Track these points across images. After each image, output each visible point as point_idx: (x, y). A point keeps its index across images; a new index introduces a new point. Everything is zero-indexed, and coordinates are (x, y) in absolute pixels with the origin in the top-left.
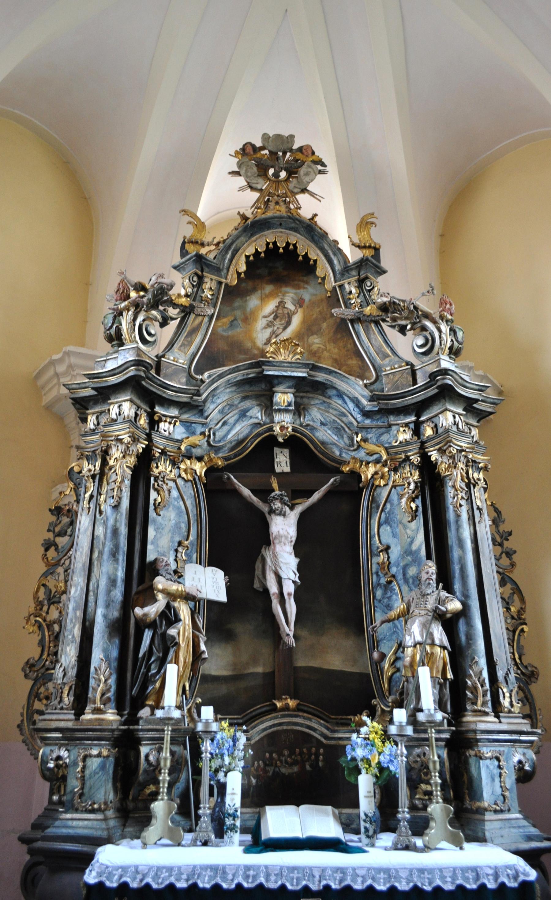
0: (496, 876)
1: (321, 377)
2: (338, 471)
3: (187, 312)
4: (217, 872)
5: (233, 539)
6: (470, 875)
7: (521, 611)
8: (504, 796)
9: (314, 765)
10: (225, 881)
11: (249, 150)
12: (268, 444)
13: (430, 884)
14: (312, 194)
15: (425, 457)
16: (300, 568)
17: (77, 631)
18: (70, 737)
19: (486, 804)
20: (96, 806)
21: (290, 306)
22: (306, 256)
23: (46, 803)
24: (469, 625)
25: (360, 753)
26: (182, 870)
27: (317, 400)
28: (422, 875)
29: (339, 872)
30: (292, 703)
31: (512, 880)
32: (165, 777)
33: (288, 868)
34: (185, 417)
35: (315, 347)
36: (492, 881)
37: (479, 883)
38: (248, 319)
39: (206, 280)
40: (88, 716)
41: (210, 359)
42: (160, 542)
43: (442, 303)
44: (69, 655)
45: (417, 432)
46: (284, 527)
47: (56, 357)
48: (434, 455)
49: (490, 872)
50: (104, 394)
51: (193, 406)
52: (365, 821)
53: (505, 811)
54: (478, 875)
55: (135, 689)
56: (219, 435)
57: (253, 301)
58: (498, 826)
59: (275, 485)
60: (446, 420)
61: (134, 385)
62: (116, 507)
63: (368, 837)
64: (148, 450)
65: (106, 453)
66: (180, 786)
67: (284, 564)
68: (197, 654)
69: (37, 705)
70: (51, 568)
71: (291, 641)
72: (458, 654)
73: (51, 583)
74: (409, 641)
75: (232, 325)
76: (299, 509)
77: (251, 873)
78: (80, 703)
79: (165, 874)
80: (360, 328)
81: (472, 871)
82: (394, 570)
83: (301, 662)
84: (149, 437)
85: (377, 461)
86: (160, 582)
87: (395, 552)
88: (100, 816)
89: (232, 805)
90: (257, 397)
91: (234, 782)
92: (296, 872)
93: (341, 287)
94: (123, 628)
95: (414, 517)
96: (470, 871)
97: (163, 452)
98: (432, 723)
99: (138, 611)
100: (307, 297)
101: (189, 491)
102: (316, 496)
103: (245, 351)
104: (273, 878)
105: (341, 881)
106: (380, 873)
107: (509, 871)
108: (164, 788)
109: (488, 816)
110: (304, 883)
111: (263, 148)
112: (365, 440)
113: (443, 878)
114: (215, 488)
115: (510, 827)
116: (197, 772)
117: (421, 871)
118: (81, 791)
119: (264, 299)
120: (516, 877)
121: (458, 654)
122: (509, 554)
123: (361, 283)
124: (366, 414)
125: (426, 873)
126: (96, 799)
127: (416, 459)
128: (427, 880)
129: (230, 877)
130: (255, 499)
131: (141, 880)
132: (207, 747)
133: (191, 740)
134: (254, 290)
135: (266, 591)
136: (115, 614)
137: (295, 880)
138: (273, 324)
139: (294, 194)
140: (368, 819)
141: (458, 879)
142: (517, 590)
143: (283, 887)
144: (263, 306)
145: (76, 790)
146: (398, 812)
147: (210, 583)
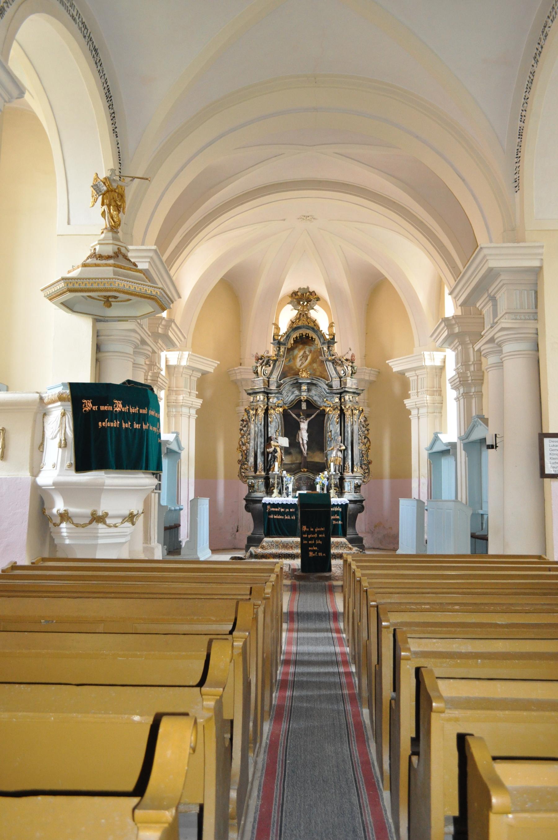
1: (314, 382)
2: (319, 409)
3: (275, 361)
5: (290, 429)
11: (294, 295)
14: (315, 310)
15: (341, 407)
16: (308, 436)
17: (253, 454)
18: (255, 478)
21: (307, 353)
22: (312, 338)
24: (347, 452)
25: (318, 481)
27: (314, 388)
30: (306, 470)
32: (276, 485)
34: (277, 395)
35: (315, 368)
38: (294, 358)
39: (281, 348)
40: (258, 473)
41: (284, 375)
42: (272, 432)
44: (252, 460)
45: (340, 399)
46: (304, 426)
47: (235, 368)
48: (343, 407)
55: (268, 467)
56: (286, 399)
57: (296, 352)
59: (301, 414)
60: (347, 397)
61: (264, 392)
62: (261, 424)
64: (267, 407)
65: (257, 410)
66: (279, 488)
67: (304, 435)
68: (282, 459)
70: (243, 436)
71: (305, 455)
72: (344, 459)
73: (243, 440)
74: (332, 456)
75: (289, 361)
76: (309, 420)
78: (256, 470)
80: (327, 363)
82: (332, 437)
83: (309, 460)
84: (267, 404)
85: (330, 406)
86: (272, 443)
87: (333, 432)
90: (297, 387)
93: (323, 348)
94: (265, 454)
95: (338, 423)
97: (271, 407)
98: (332, 474)
99: (268, 450)
100: (313, 349)
101: (278, 417)
102: (313, 416)
108: (276, 487)
111: (298, 292)
112: (327, 400)
114: (285, 415)
116: (283, 484)
119: (300, 350)
121: (344, 459)
122: (368, 430)
124: (328, 393)
127: (339, 408)
130: (296, 418)
132: (284, 479)
134: (296, 347)
135: (299, 442)
136: (262, 450)
138: (301, 359)
139: (309, 310)
142: (369, 440)
144: (299, 353)
147: (284, 442)
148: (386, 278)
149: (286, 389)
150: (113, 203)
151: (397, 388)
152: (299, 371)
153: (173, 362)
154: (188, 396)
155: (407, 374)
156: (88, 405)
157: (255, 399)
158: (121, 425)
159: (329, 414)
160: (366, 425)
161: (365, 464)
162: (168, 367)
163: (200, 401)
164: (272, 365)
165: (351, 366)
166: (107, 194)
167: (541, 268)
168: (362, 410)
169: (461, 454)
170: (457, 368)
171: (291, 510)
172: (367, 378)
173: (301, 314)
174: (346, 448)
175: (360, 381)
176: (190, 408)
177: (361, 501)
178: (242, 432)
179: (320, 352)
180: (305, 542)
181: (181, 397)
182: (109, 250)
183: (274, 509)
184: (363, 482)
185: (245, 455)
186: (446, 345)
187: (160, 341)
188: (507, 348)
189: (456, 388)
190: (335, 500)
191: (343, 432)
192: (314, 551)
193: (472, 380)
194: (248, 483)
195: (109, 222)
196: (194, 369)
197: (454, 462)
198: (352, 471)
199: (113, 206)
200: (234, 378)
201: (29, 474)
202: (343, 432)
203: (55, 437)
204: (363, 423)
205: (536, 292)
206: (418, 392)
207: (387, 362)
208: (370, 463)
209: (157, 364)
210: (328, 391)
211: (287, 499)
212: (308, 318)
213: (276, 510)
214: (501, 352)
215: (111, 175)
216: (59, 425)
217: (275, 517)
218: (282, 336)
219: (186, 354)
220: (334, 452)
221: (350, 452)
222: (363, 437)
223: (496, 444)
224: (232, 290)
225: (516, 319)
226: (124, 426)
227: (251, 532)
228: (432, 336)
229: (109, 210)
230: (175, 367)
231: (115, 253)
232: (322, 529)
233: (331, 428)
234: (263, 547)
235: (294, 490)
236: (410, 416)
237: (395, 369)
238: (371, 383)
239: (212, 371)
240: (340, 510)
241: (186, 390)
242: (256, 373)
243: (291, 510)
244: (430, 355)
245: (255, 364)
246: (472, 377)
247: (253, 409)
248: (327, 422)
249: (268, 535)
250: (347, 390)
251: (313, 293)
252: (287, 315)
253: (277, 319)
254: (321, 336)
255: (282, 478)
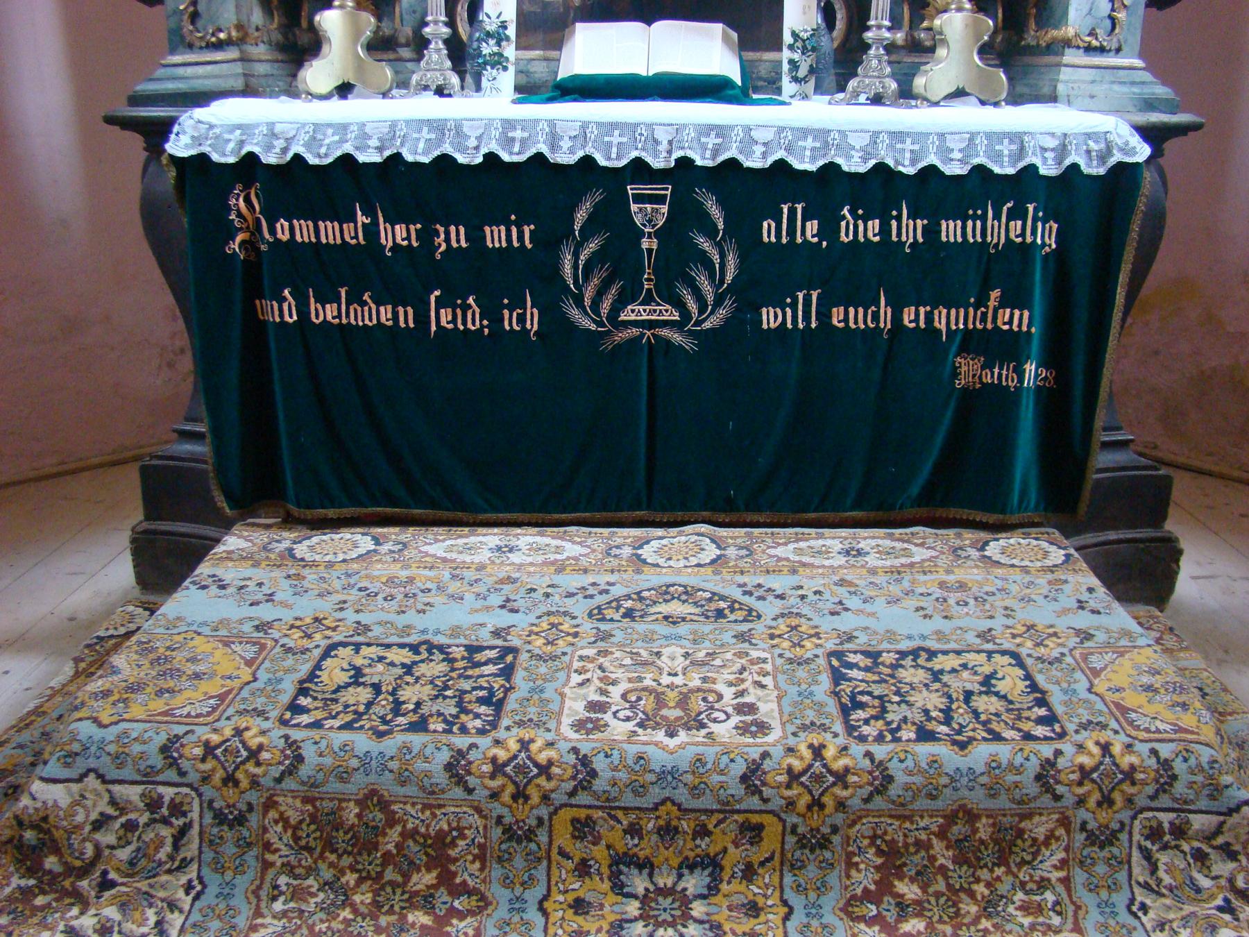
0: (1062, 151)
4: (444, 135)
6: (1006, 148)
8: (1113, 20)
10: (463, 150)
13: (913, 162)
19: (1071, 32)
20: (222, 36)
26: (367, 130)
28: (899, 146)
29: (713, 134)
31: (1095, 163)
33: (599, 124)
36: (1050, 162)
37: (1021, 165)
49: (1052, 143)
52: (791, 47)
53: (1110, 50)
54: (1022, 148)
58: (1089, 78)
63: (796, 80)
77: (518, 134)
79: (331, 138)
81: (1011, 141)
88: (233, 53)
89: (493, 15)
92: (617, 133)
96: (1006, 141)
104: (566, 144)
105: (716, 151)
106: (805, 138)
107: (1091, 143)
109: (1070, 56)
110: (635, 154)
113: (945, 152)
115: (1113, 82)
117: (898, 136)
118: (191, 9)
120: (1102, 158)
125: (909, 141)
126: (222, 23)
128: (908, 155)
129: (472, 143)
131: (285, 150)
137: (614, 150)
140: (799, 44)
141: (978, 156)
143: (588, 161)
145: (182, 7)
146: (868, 28)
171: (495, 237)
183: (304, 231)
213: (330, 232)
243: (495, 237)
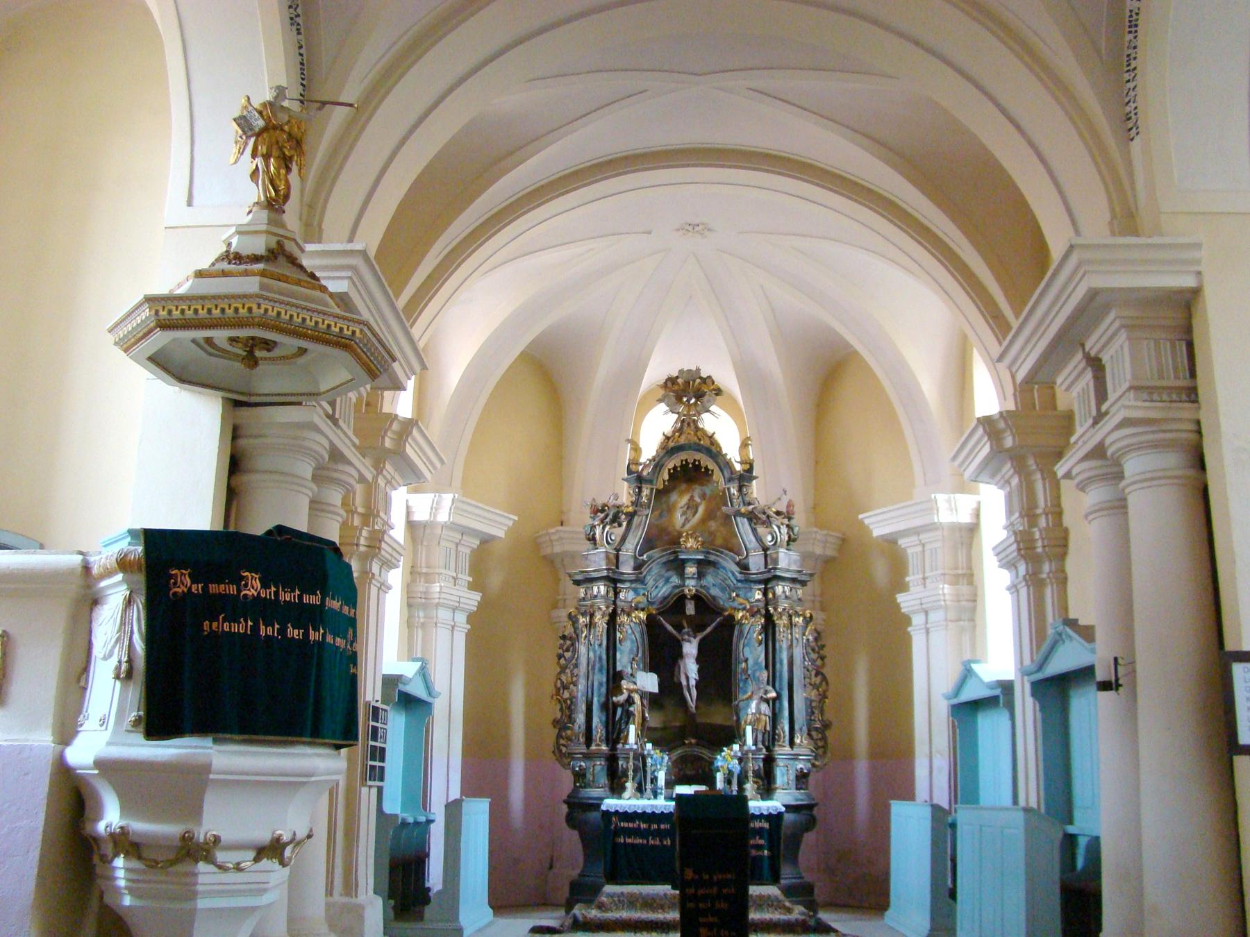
1: (712, 558)
3: (631, 516)
5: (661, 655)
7: (825, 692)
9: (704, 771)
11: (669, 384)
12: (682, 599)
14: (713, 414)
16: (700, 671)
17: (584, 707)
18: (587, 757)
21: (697, 499)
22: (706, 468)
23: (572, 786)
24: (781, 704)
25: (720, 764)
27: (711, 570)
30: (693, 741)
32: (631, 773)
38: (671, 510)
40: (593, 747)
42: (623, 661)
43: (789, 505)
44: (581, 719)
45: (765, 594)
46: (690, 648)
48: (771, 609)
50: (592, 580)
51: (640, 580)
55: (615, 735)
57: (674, 497)
62: (600, 645)
64: (614, 611)
65: (592, 616)
66: (637, 778)
67: (690, 669)
69: (562, 742)
70: (563, 669)
71: (693, 710)
72: (775, 718)
73: (564, 678)
75: (661, 516)
80: (738, 519)
83: (699, 720)
84: (615, 603)
85: (744, 609)
86: (623, 682)
87: (750, 662)
90: (675, 569)
91: (662, 777)
94: (609, 708)
95: (760, 644)
98: (750, 751)
101: (637, 630)
102: (709, 629)
103: (669, 534)
108: (631, 777)
114: (651, 625)
116: (645, 772)
119: (681, 494)
121: (775, 718)
122: (822, 658)
123: (740, 490)
130: (674, 632)
132: (649, 761)
133: (641, 758)
134: (674, 488)
136: (603, 699)
138: (684, 513)
139: (700, 414)
142: (824, 679)
144: (680, 500)
147: (649, 682)
148: (856, 353)
149: (653, 573)
150: (275, 153)
151: (880, 570)
152: (680, 535)
153: (421, 515)
154: (451, 585)
155: (902, 542)
156: (183, 582)
157: (589, 592)
158: (255, 629)
159: (741, 625)
160: (818, 647)
161: (816, 729)
162: (411, 525)
163: (477, 596)
164: (625, 524)
165: (788, 526)
166: (265, 135)
167: (1196, 292)
168: (811, 617)
169: (1025, 704)
170: (1012, 524)
171: (662, 826)
172: (818, 550)
173: (683, 421)
174: (779, 697)
175: (805, 557)
176: (454, 609)
177: (810, 807)
178: (562, 661)
179: (723, 498)
180: (691, 905)
181: (436, 588)
182: (258, 245)
183: (626, 825)
184: (814, 765)
185: (568, 708)
186: (983, 477)
187: (388, 466)
188: (1133, 466)
189: (1009, 565)
190: (757, 805)
191: (771, 662)
192: (710, 926)
193: (1044, 547)
194: (573, 768)
195: (265, 191)
196: (465, 531)
197: (1009, 723)
198: (792, 744)
199: (277, 158)
200: (549, 551)
201: (51, 738)
202: (771, 662)
203: (111, 655)
204: (813, 644)
205: (1190, 345)
206: (924, 579)
207: (860, 517)
208: (826, 726)
209: (382, 514)
210: (739, 576)
211: (653, 802)
212: (697, 429)
213: (631, 825)
214: (1120, 476)
215: (276, 98)
216: (116, 627)
217: (629, 841)
218: (646, 466)
219: (447, 499)
220: (753, 705)
221: (786, 704)
222: (813, 673)
223: (1117, 679)
224: (546, 375)
225: (1152, 401)
226: (263, 633)
227: (578, 871)
228: (954, 458)
229: (268, 166)
230: (424, 525)
231: (271, 251)
232: (729, 876)
233: (747, 652)
234: (601, 907)
235: (670, 784)
236: (909, 629)
237: (877, 532)
238: (828, 562)
239: (501, 534)
240: (766, 825)
241: (443, 571)
242: (592, 539)
243: (662, 826)
244: (949, 501)
245: (591, 522)
246: (1043, 539)
247: (584, 615)
248: (738, 641)
249: (613, 878)
250: (779, 573)
251: (707, 381)
252: (656, 426)
253: (636, 432)
254: (725, 464)
255: (644, 758)
